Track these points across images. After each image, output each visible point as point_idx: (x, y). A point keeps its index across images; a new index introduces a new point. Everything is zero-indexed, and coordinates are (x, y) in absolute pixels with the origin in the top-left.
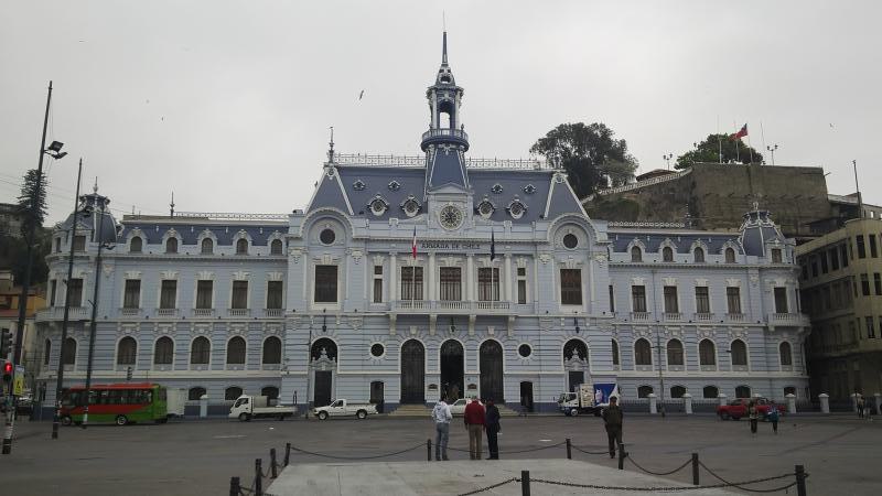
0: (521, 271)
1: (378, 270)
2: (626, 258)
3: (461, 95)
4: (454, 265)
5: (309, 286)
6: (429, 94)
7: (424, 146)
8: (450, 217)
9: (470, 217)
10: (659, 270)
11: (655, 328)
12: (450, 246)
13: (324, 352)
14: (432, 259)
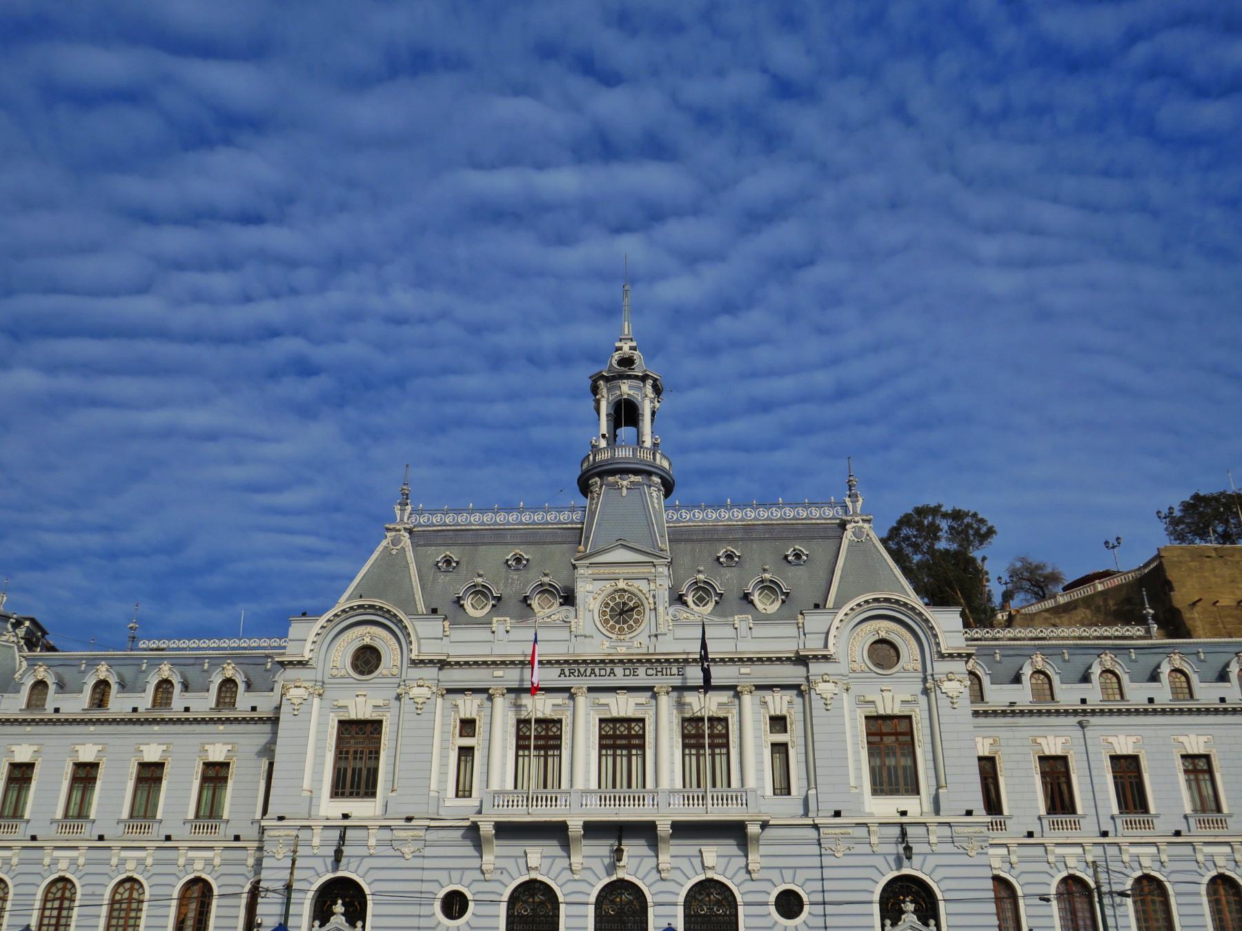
0: (778, 723)
1: (468, 726)
2: (1023, 695)
4: (631, 713)
5: (319, 764)
7: (585, 488)
8: (623, 612)
9: (661, 609)
10: (1094, 720)
13: (339, 908)
14: (581, 701)
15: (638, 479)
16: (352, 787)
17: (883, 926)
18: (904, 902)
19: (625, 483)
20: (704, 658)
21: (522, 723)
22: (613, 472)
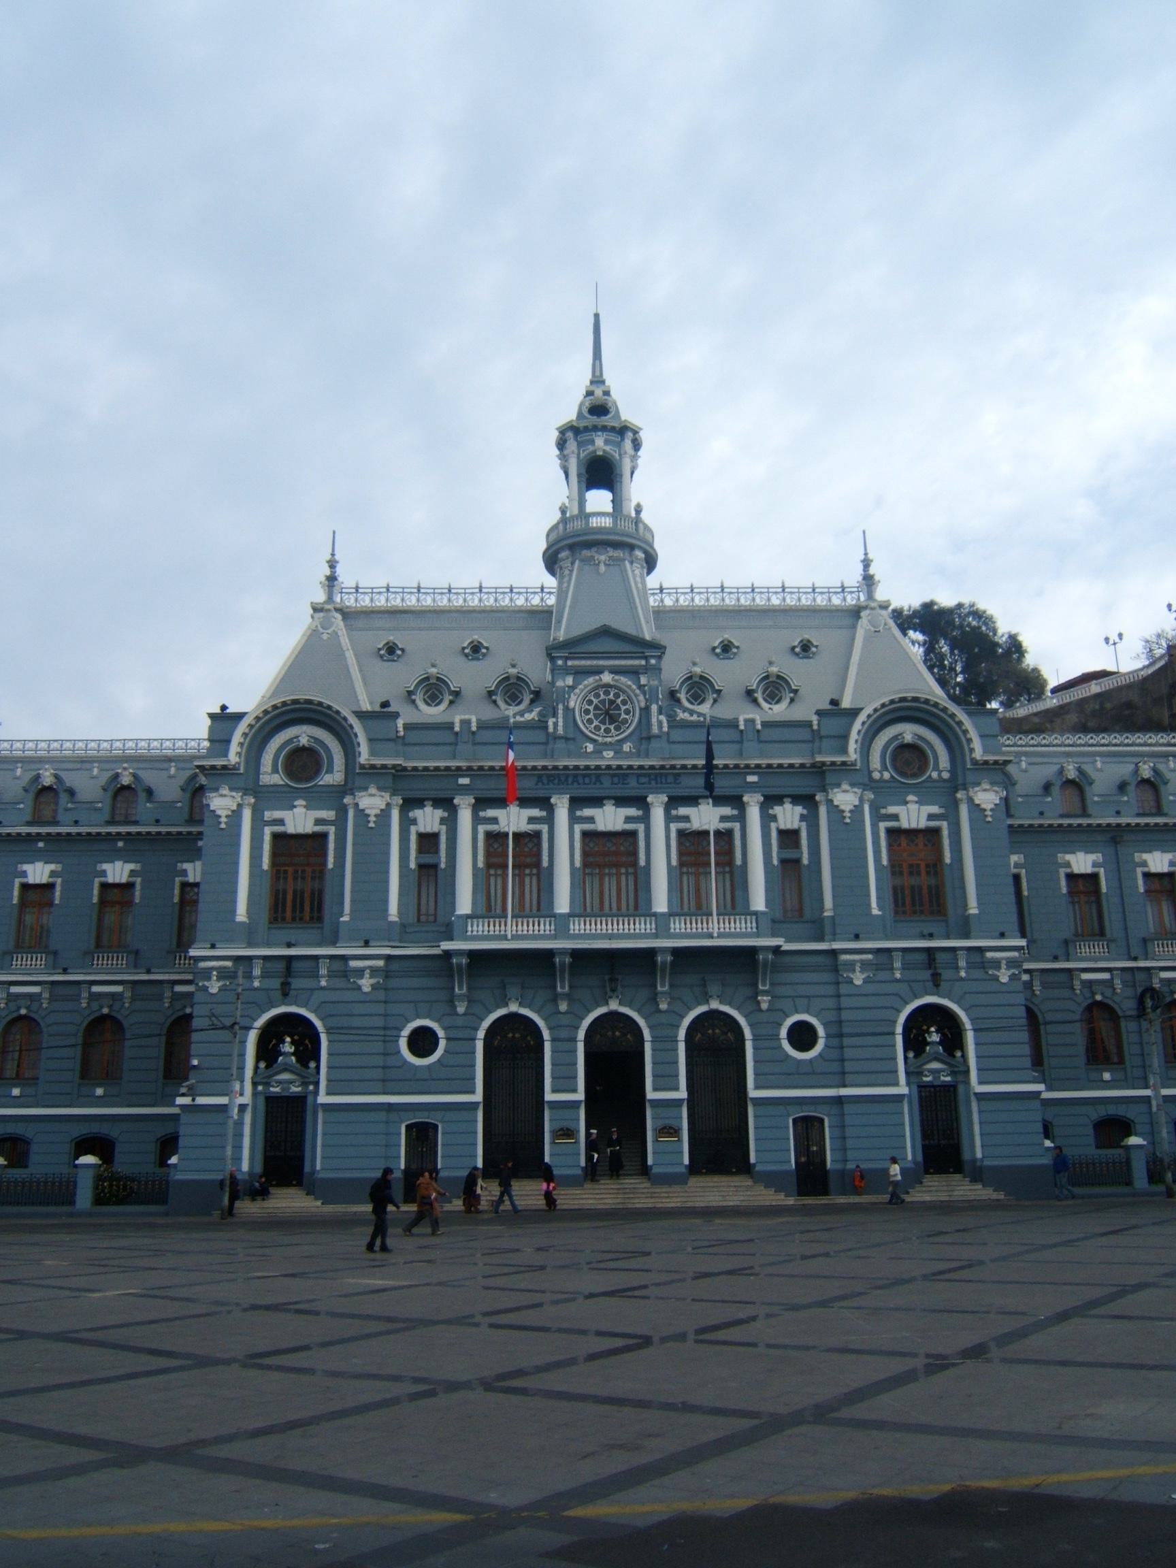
0: (789, 837)
3: (637, 445)
6: (561, 444)
7: (551, 561)
11: (1128, 976)
12: (607, 782)
13: (288, 1047)
15: (618, 553)
16: (294, 911)
17: (906, 1058)
18: (930, 1033)
19: (603, 558)
20: (710, 767)
21: (496, 839)
22: (589, 545)
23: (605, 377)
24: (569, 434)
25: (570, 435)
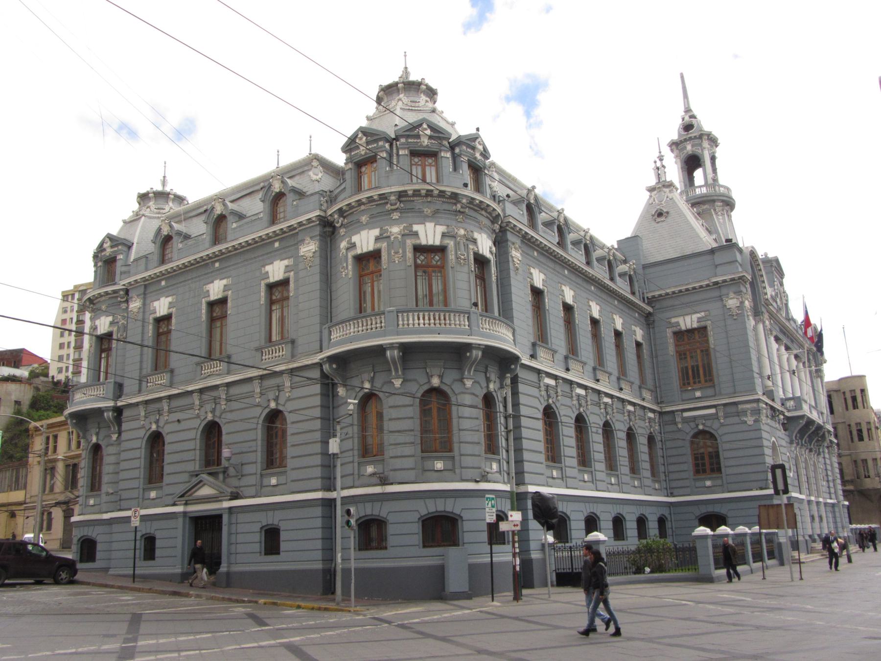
3: (713, 141)
6: (672, 151)
23: (692, 107)
24: (675, 145)
25: (674, 147)
